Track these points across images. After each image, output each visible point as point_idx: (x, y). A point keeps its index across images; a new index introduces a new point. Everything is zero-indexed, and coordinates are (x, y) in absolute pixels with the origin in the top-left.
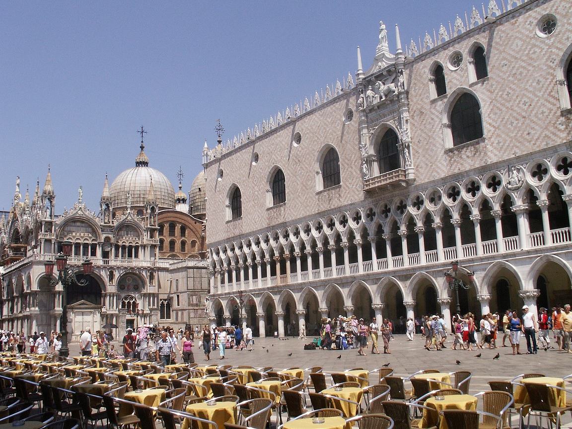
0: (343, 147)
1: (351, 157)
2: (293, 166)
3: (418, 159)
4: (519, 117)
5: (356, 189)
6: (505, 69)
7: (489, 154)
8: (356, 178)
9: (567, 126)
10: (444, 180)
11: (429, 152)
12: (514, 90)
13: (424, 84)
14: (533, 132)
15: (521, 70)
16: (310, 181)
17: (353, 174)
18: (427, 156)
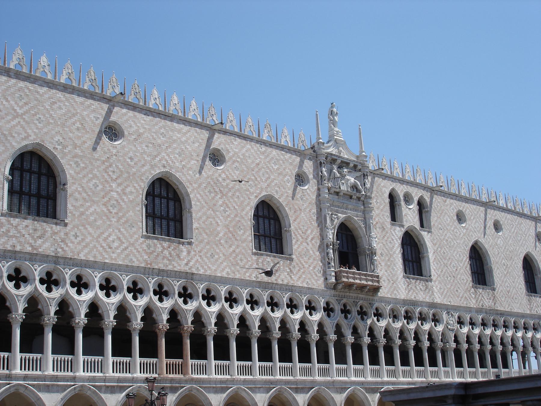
0: (295, 212)
1: (306, 230)
2: (210, 192)
3: (381, 271)
4: (451, 275)
5: (315, 272)
6: (441, 231)
7: (435, 294)
8: (314, 260)
9: (475, 296)
10: (405, 302)
11: (390, 269)
12: (447, 252)
13: (384, 202)
14: (459, 291)
15: (450, 240)
16: (242, 231)
17: (309, 252)
18: (388, 271)
